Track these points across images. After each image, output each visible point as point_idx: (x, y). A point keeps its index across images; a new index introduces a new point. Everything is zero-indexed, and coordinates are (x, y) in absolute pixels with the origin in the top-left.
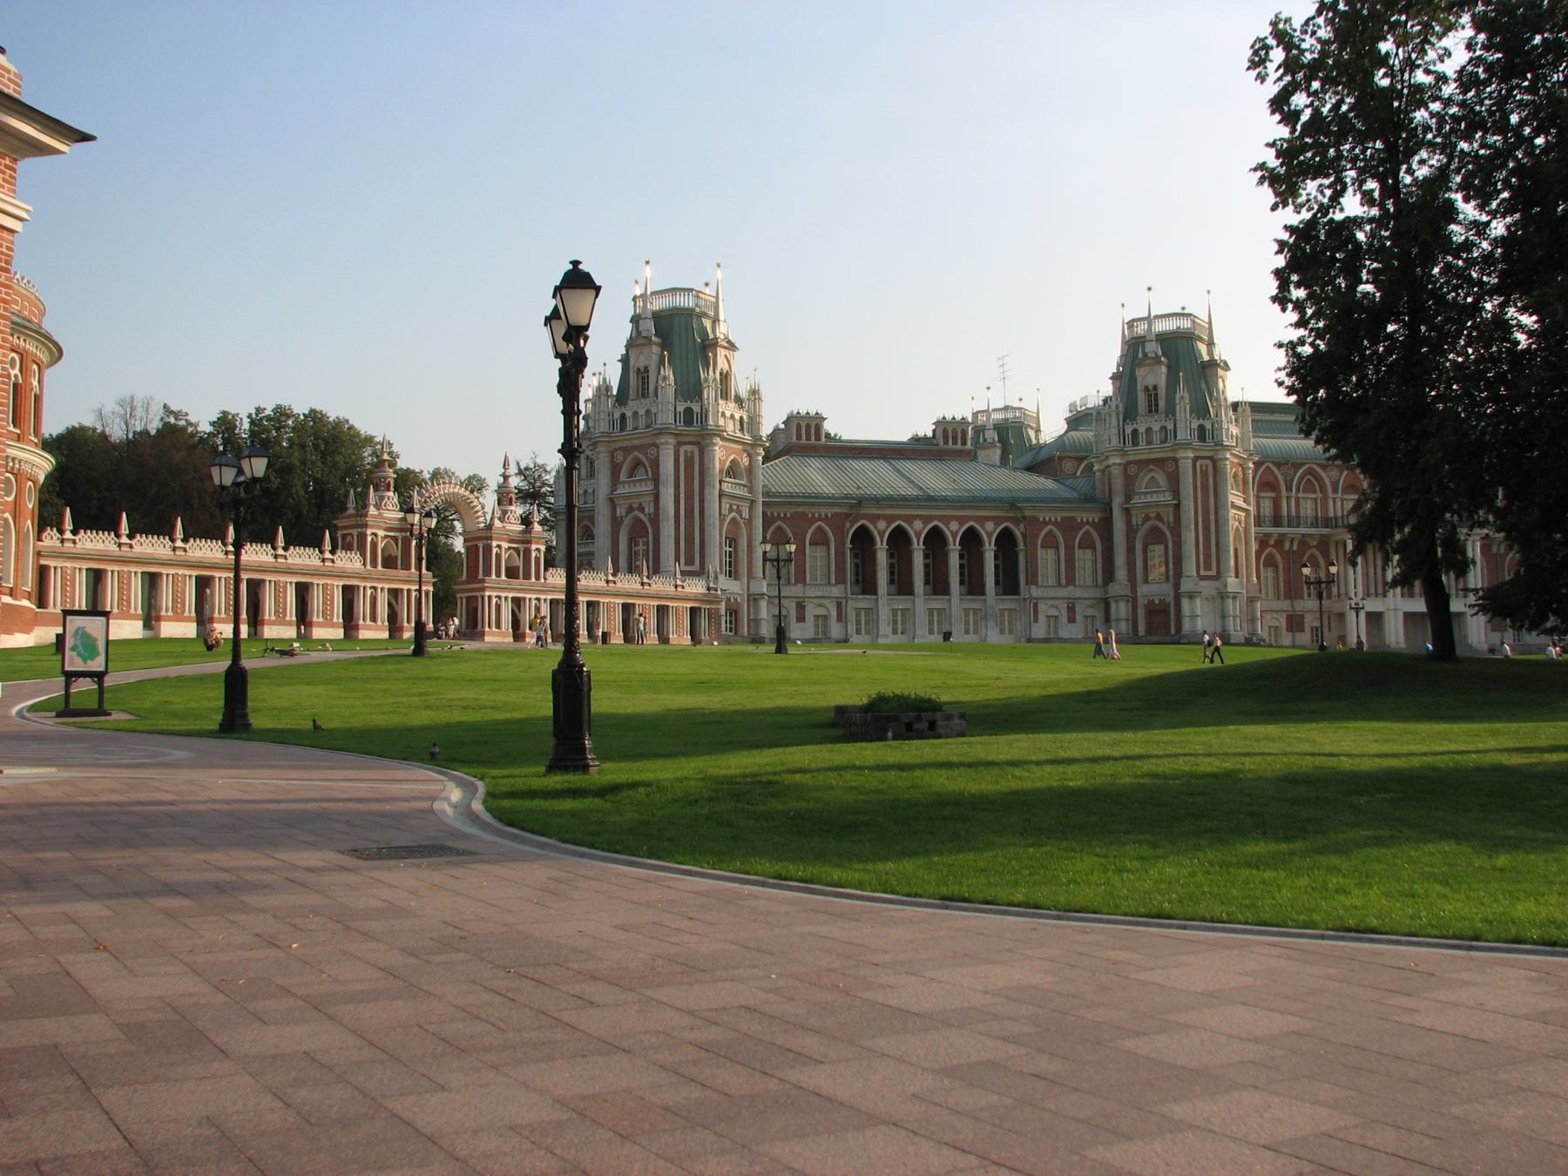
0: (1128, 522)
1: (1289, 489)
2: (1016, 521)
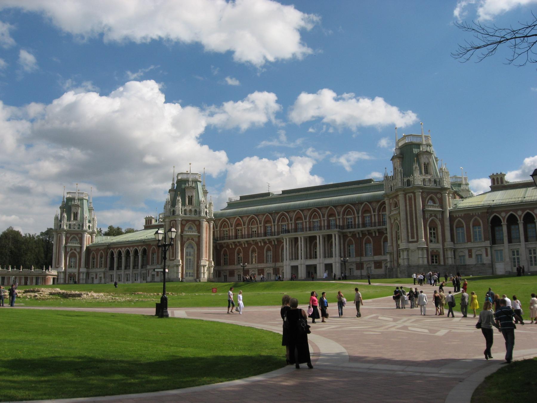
1: (274, 222)
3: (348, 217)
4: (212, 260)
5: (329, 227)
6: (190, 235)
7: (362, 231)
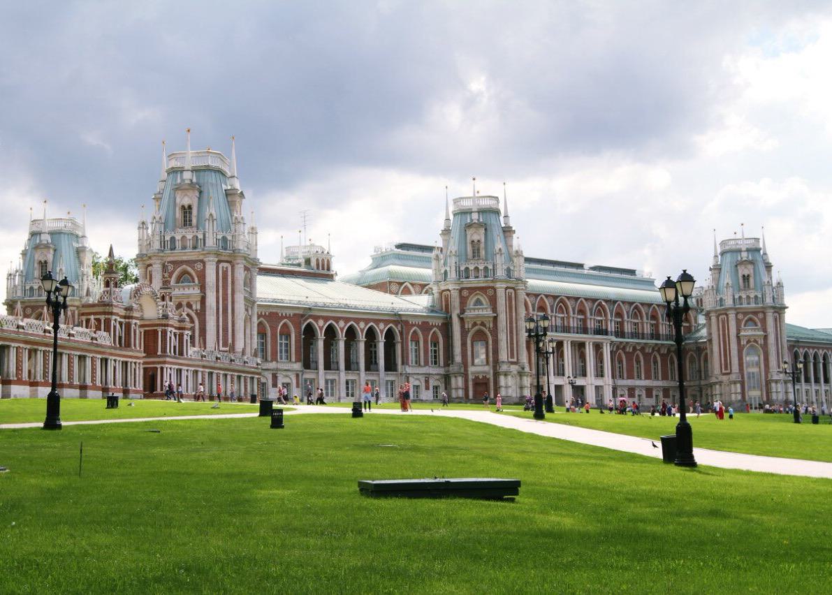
0: (462, 327)
2: (396, 323)
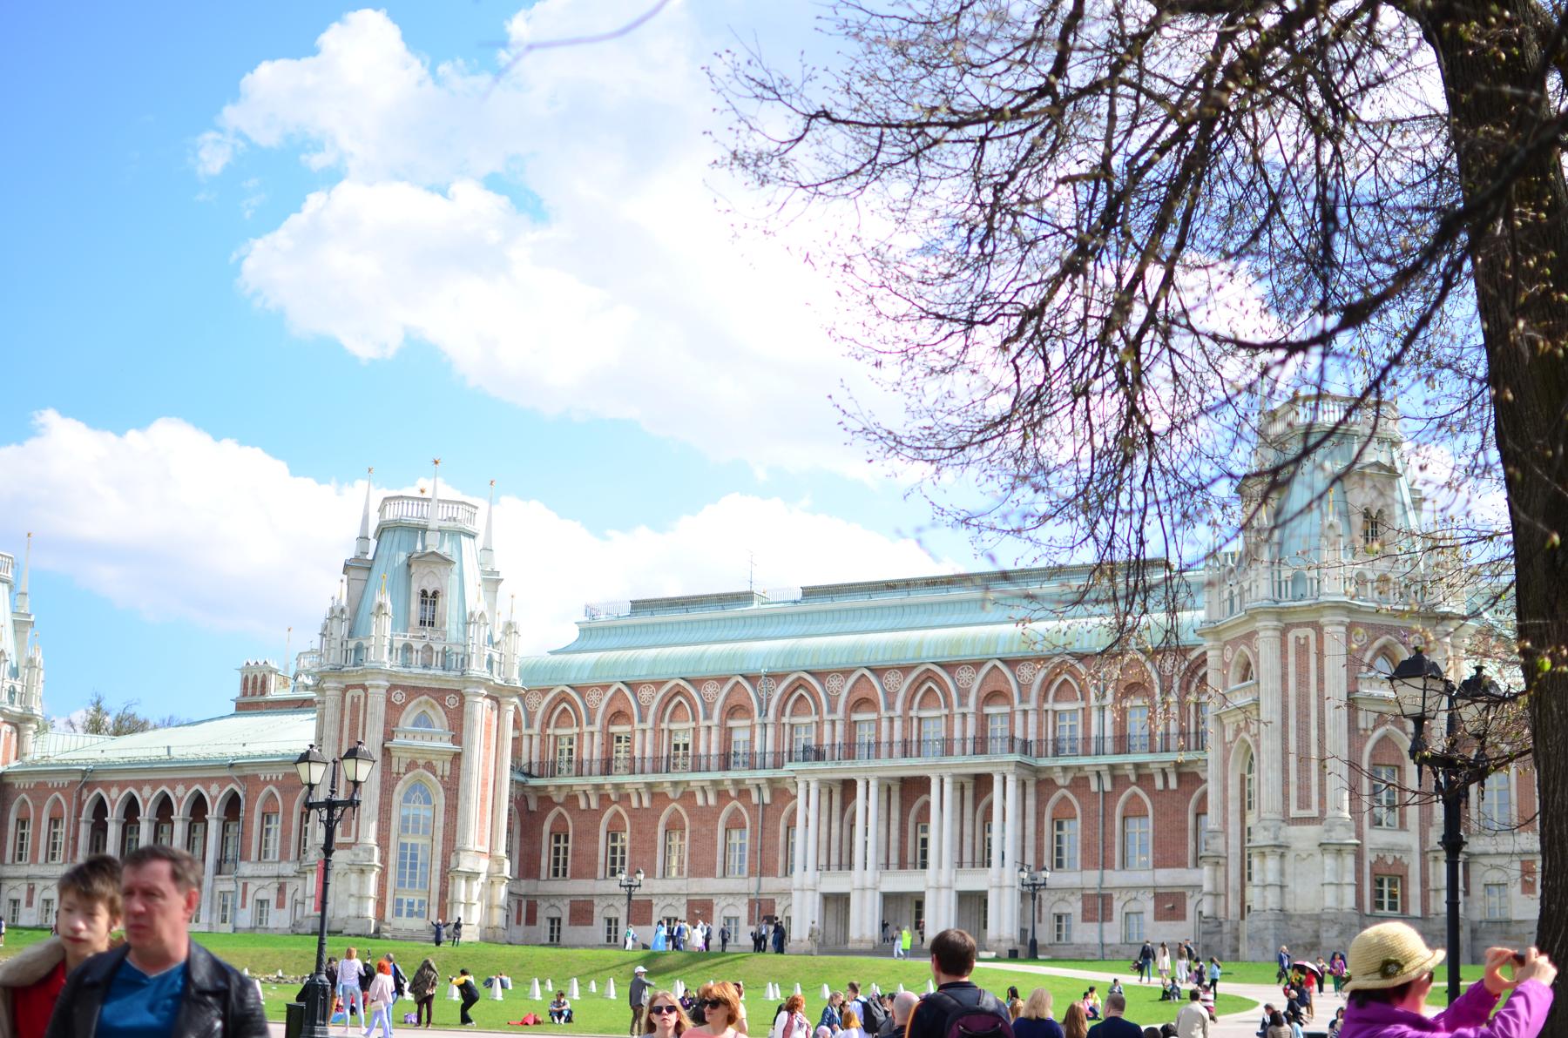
1: (764, 712)
3: (1059, 707)
4: (502, 852)
5: (981, 744)
6: (422, 751)
7: (1112, 767)
